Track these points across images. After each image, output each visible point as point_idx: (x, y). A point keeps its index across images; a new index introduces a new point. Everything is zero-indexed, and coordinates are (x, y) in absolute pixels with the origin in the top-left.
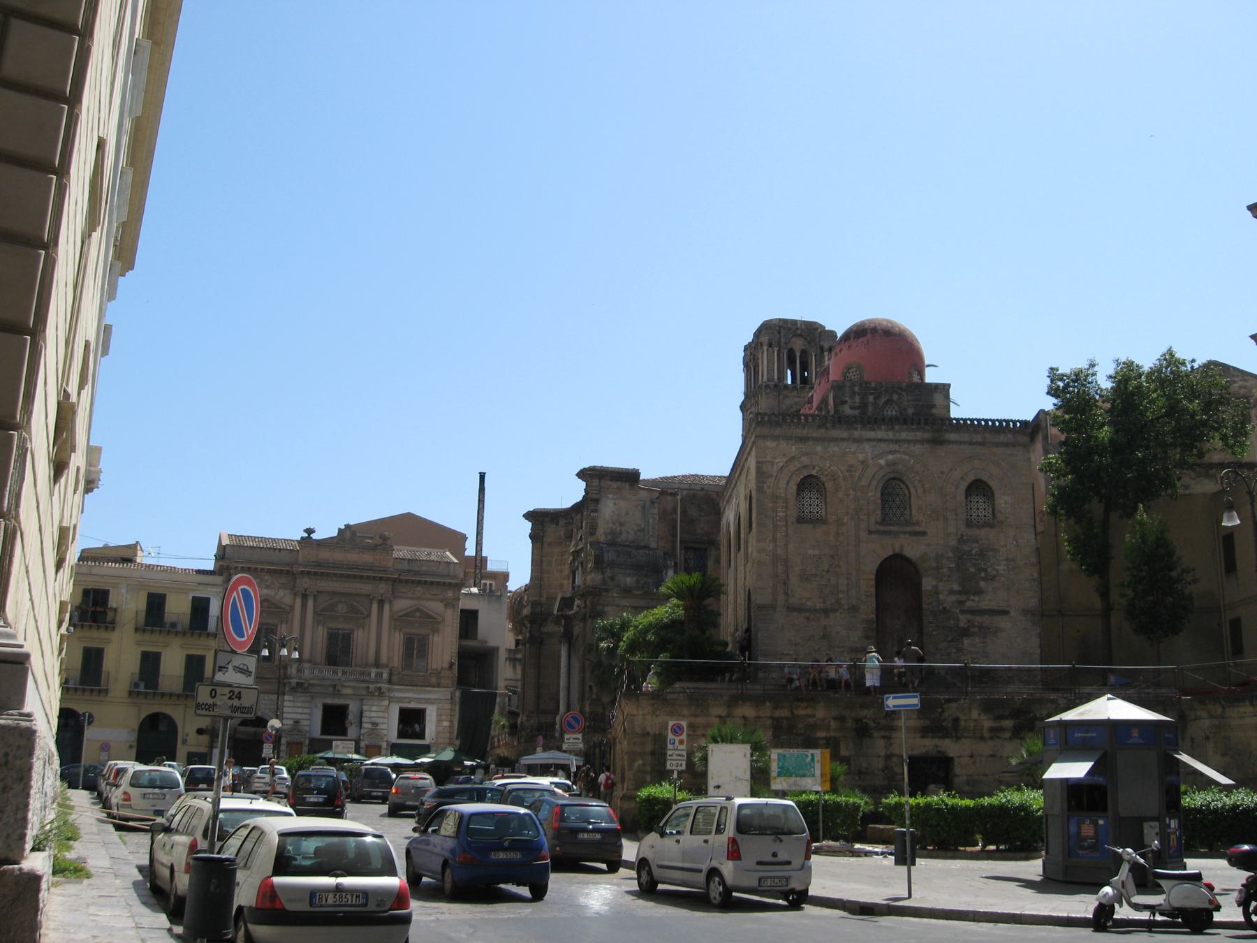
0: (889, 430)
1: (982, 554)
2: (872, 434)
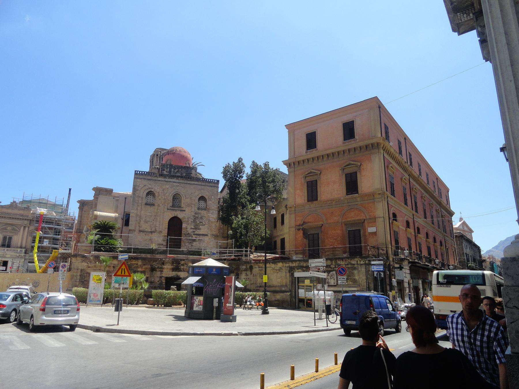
1: (201, 218)
2: (171, 180)
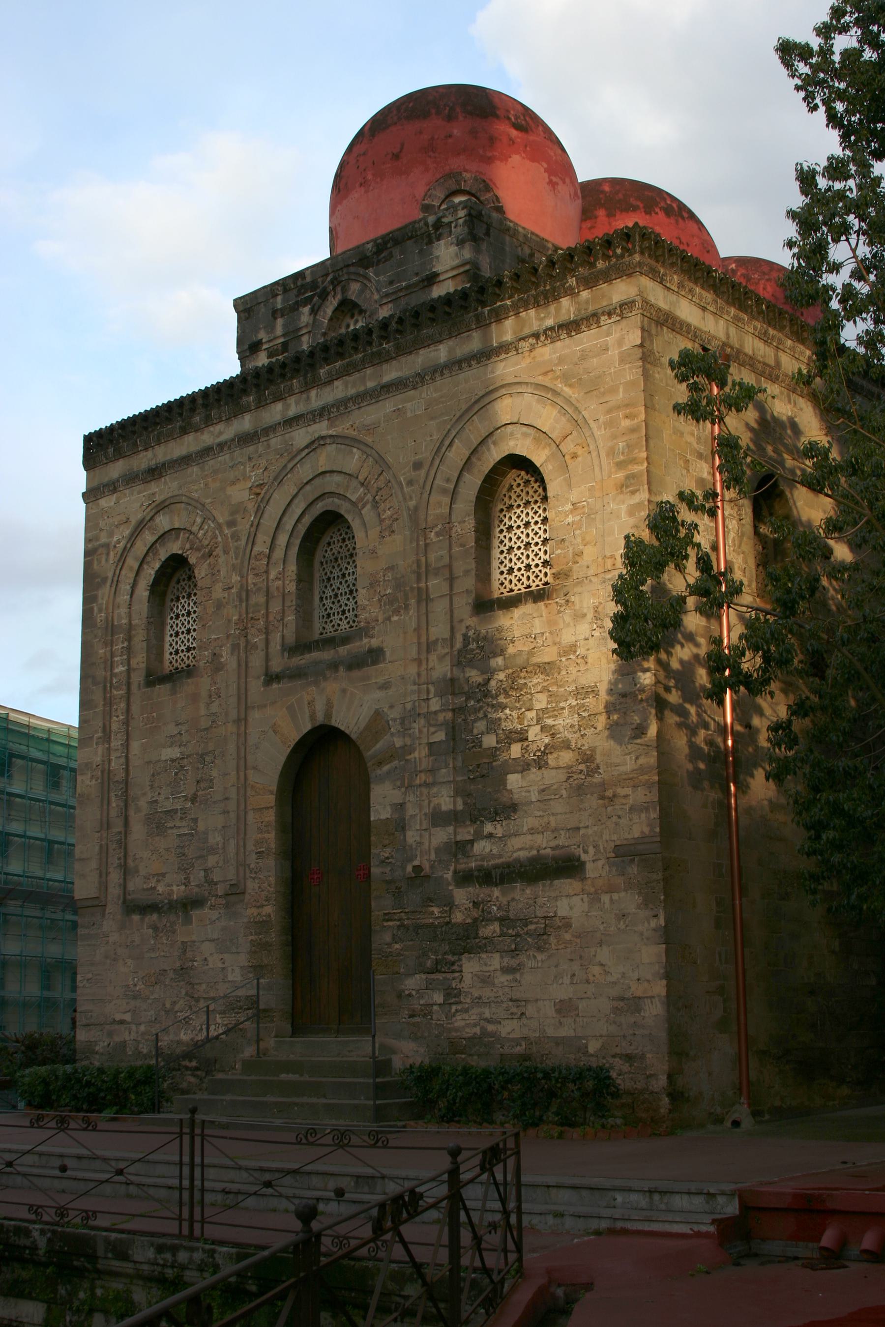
0: (307, 387)
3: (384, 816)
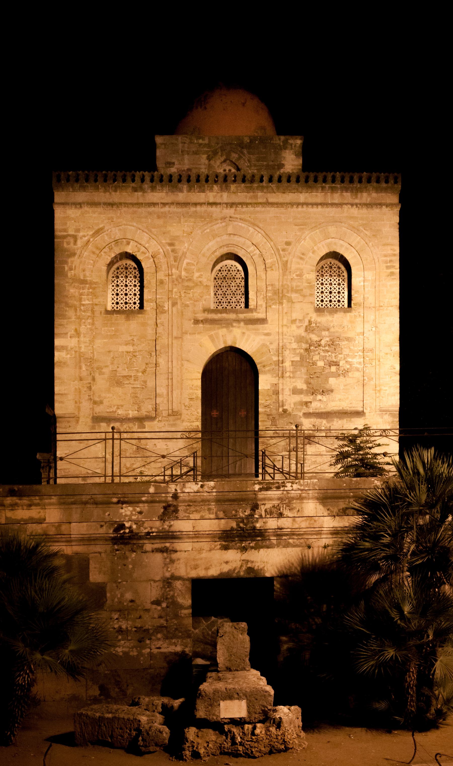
0: (222, 190)
3: (266, 388)
